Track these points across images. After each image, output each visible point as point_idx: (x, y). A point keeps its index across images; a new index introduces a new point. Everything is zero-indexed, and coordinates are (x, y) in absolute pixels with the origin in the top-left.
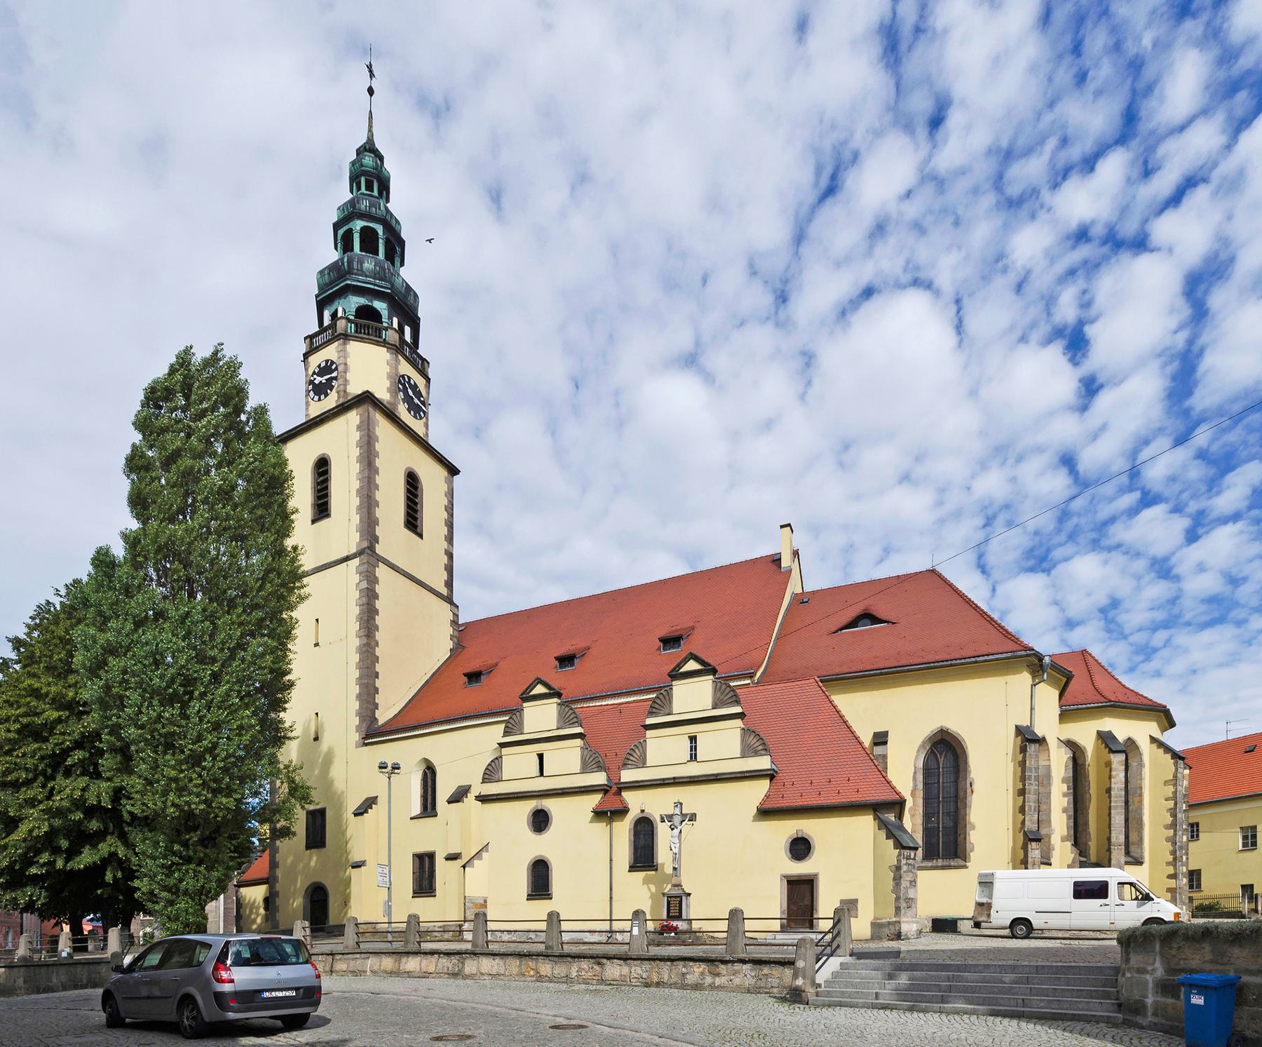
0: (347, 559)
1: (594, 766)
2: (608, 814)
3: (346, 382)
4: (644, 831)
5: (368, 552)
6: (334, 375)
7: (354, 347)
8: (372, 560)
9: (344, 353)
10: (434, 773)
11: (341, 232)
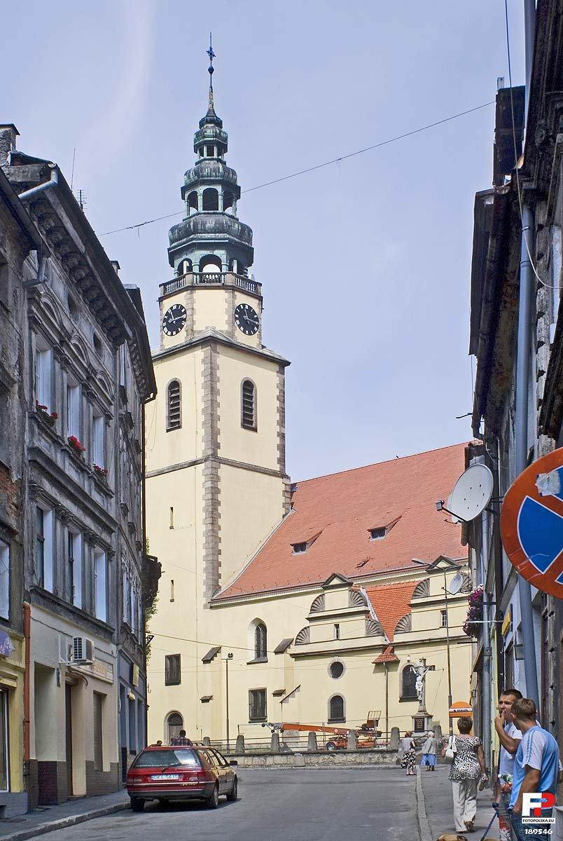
0: (194, 463)
1: (376, 632)
2: (385, 665)
4: (409, 676)
5: (214, 459)
6: (184, 316)
7: (198, 294)
8: (215, 464)
10: (265, 630)
11: (187, 195)
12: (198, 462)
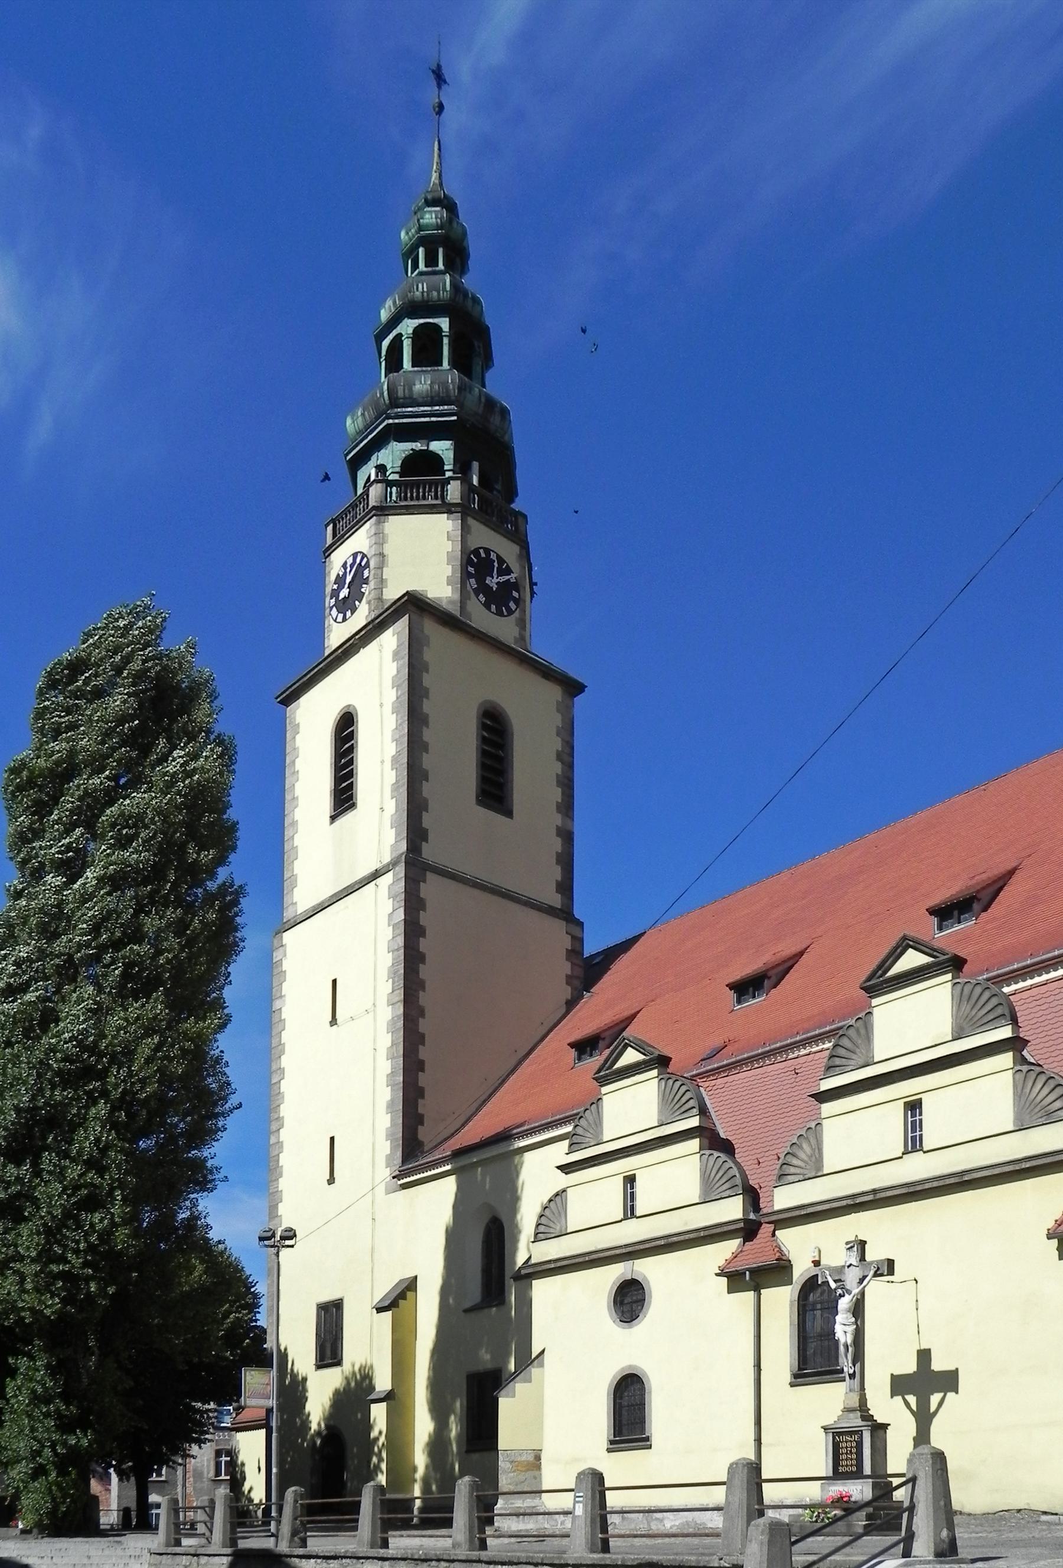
0: (376, 875)
3: (382, 583)
7: (397, 525)
9: (379, 538)
12: (383, 871)
